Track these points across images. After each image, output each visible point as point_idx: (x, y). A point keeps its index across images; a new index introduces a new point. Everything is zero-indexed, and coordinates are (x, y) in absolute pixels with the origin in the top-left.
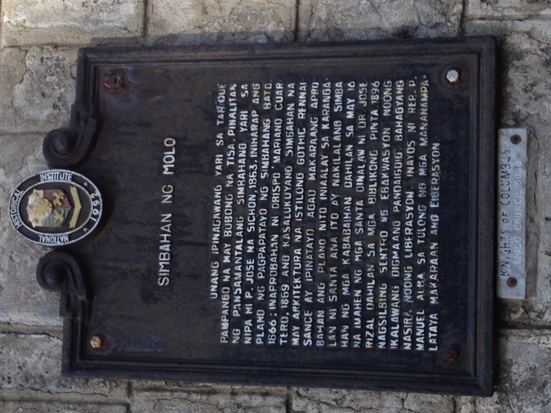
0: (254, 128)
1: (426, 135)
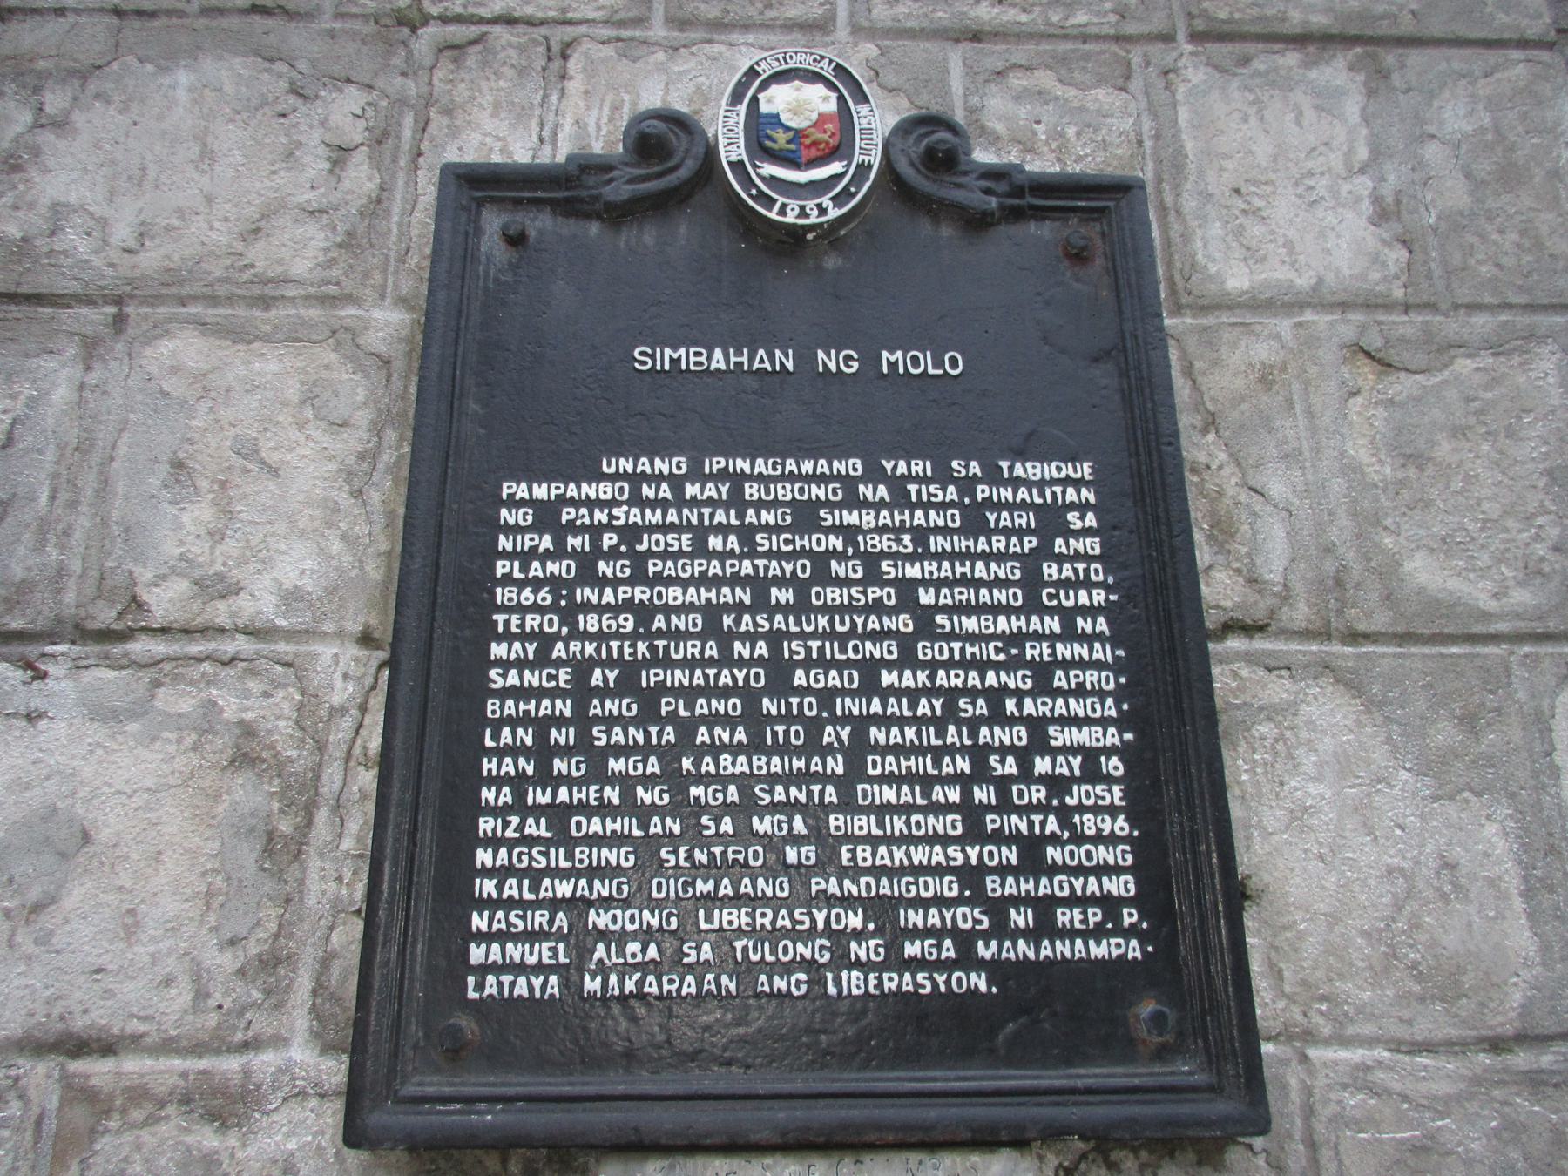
0: (999, 543)
1: (1004, 955)
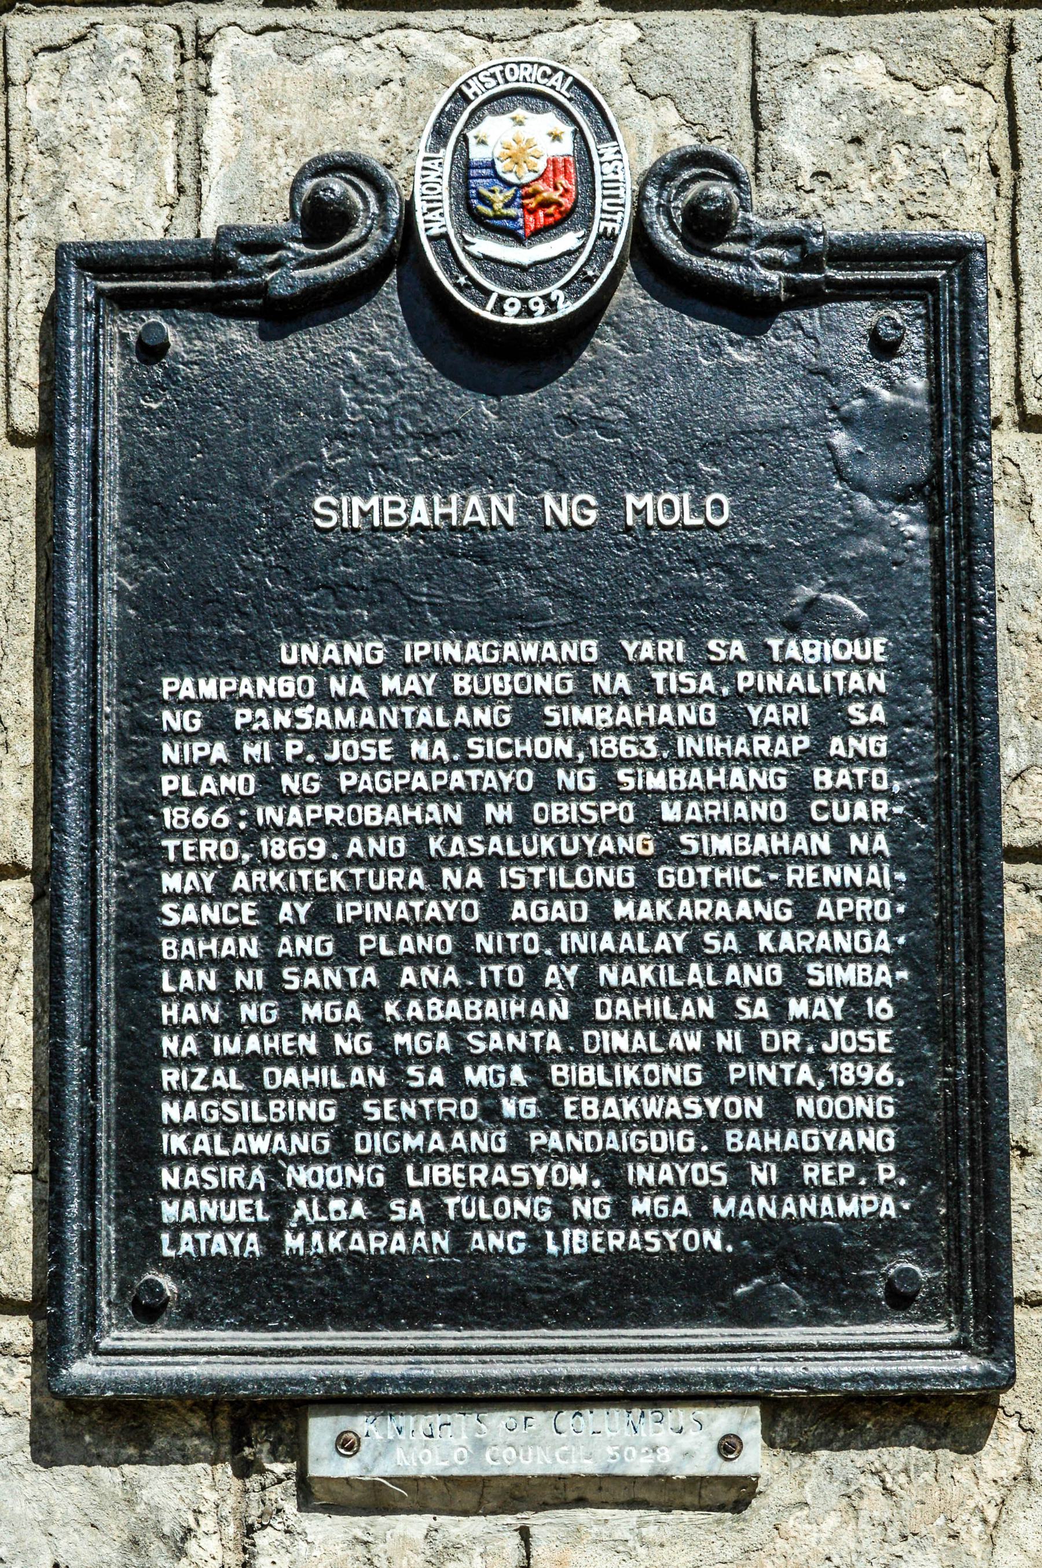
0: (762, 745)
1: (742, 1212)
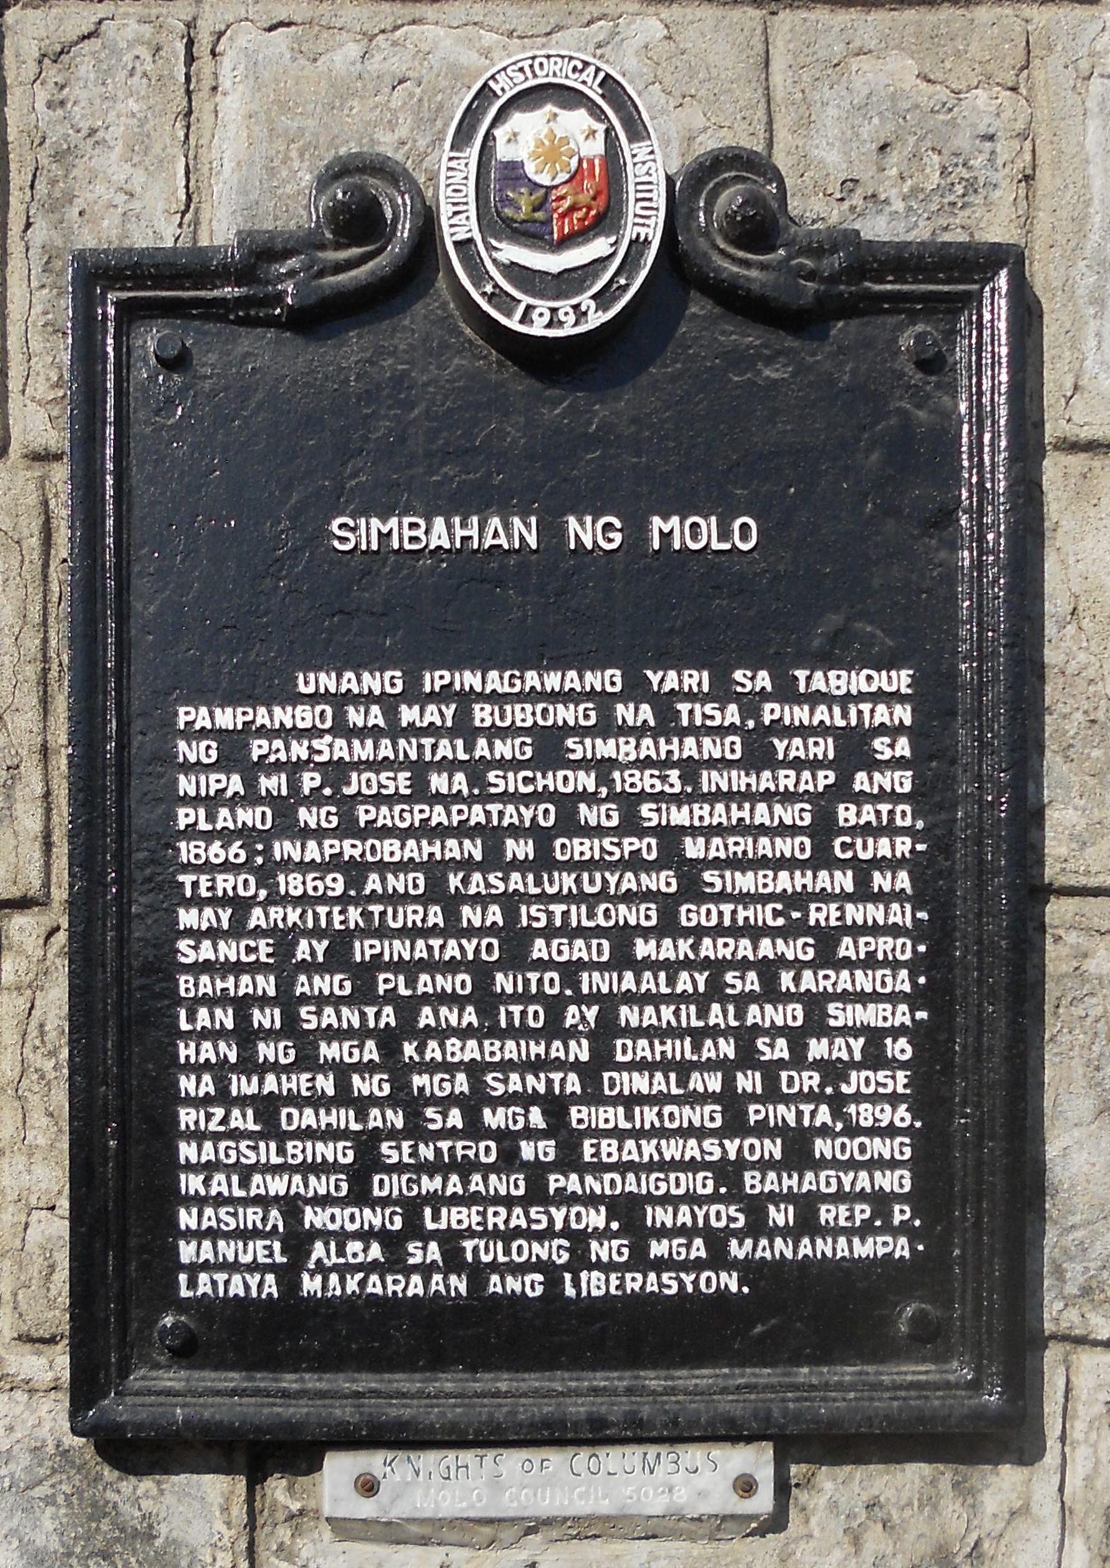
0: (787, 779)
1: (759, 1254)
